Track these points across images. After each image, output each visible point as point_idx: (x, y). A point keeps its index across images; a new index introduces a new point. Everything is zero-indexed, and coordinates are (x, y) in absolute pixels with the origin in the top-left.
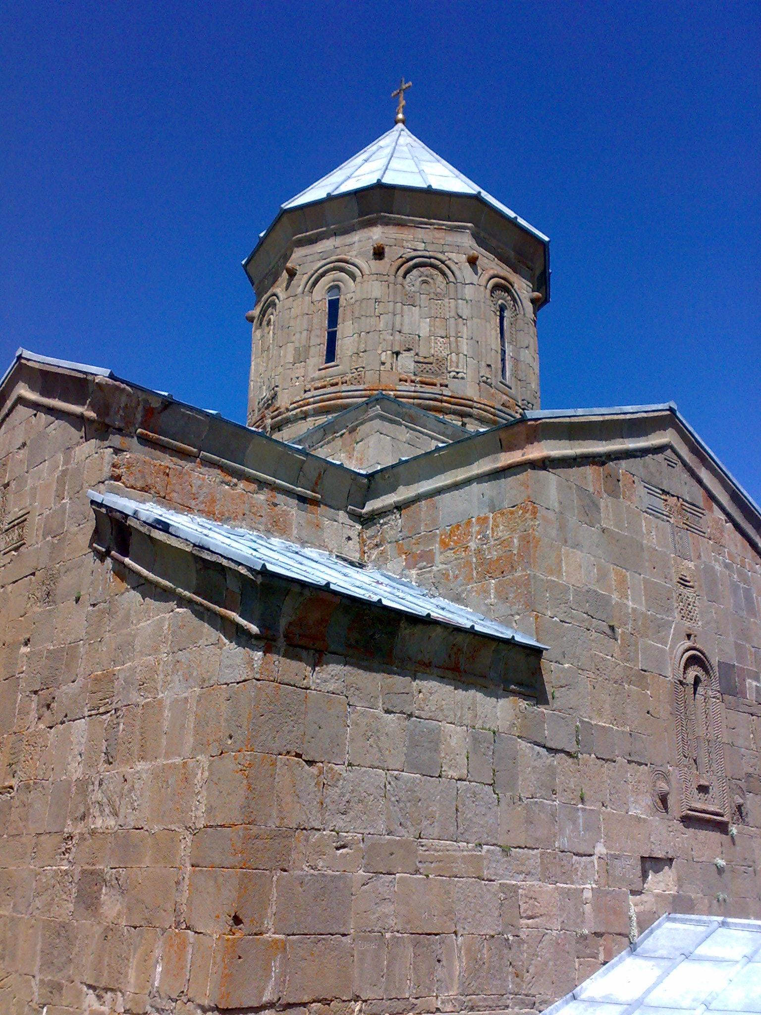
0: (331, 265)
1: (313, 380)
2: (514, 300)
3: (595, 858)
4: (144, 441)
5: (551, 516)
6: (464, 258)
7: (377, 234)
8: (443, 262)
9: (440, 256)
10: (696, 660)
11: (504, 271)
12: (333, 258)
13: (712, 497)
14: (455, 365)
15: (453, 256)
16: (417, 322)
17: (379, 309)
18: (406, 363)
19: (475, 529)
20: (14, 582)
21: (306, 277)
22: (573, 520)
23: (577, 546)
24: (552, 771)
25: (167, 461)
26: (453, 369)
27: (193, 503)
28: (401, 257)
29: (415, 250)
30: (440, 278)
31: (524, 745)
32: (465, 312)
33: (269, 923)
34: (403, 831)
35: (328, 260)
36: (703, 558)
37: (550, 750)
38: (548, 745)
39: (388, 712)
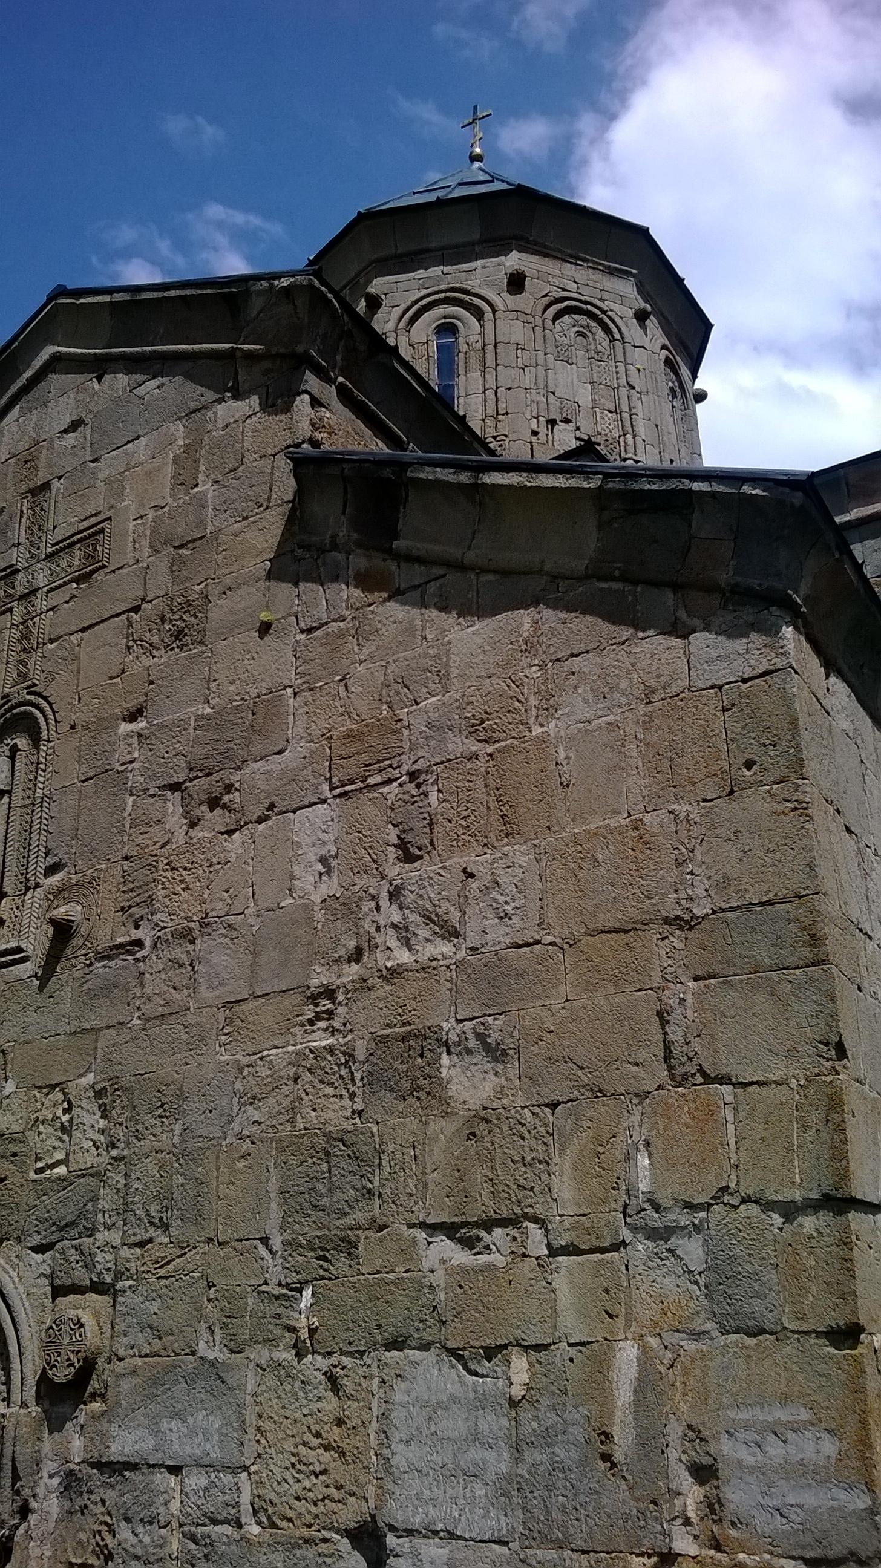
0: (442, 295)
6: (630, 313)
7: (514, 260)
8: (604, 312)
9: (599, 303)
12: (443, 287)
15: (616, 307)
16: (572, 383)
17: (525, 358)
20: (84, 630)
21: (398, 311)
26: (629, 455)
28: (546, 295)
29: (564, 290)
30: (600, 333)
35: (436, 289)
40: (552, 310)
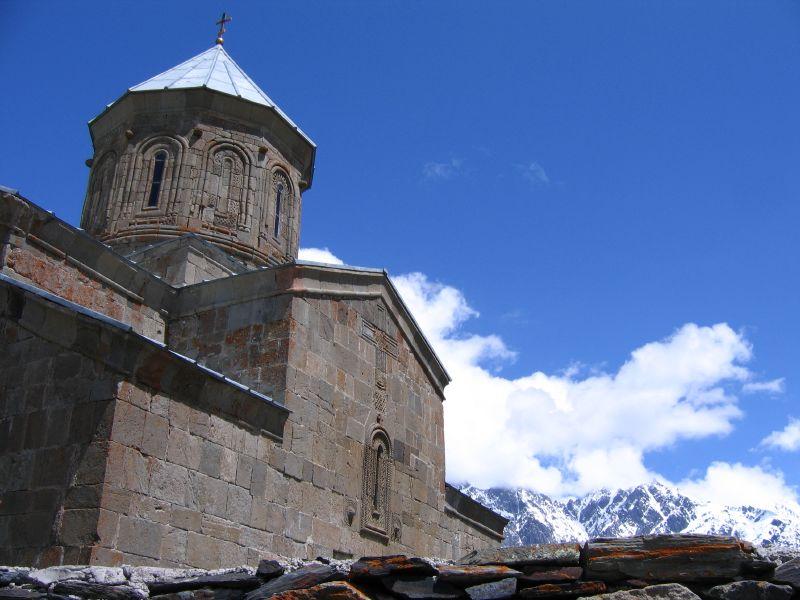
1: (137, 217)
2: (288, 182)
3: (306, 545)
4: (30, 241)
5: (303, 329)
9: (241, 144)
10: (381, 435)
11: (284, 162)
13: (403, 335)
14: (243, 221)
16: (218, 186)
18: (209, 215)
19: (252, 333)
22: (316, 335)
23: (317, 351)
24: (286, 489)
25: (45, 258)
27: (58, 290)
31: (270, 470)
32: (254, 185)
33: (114, 543)
34: (195, 507)
36: (394, 373)
37: (286, 475)
38: (287, 472)
39: (192, 434)
40: (213, 149)
